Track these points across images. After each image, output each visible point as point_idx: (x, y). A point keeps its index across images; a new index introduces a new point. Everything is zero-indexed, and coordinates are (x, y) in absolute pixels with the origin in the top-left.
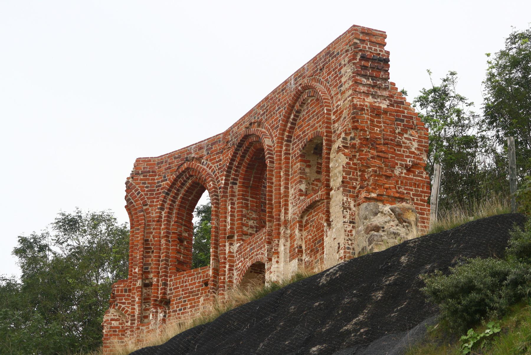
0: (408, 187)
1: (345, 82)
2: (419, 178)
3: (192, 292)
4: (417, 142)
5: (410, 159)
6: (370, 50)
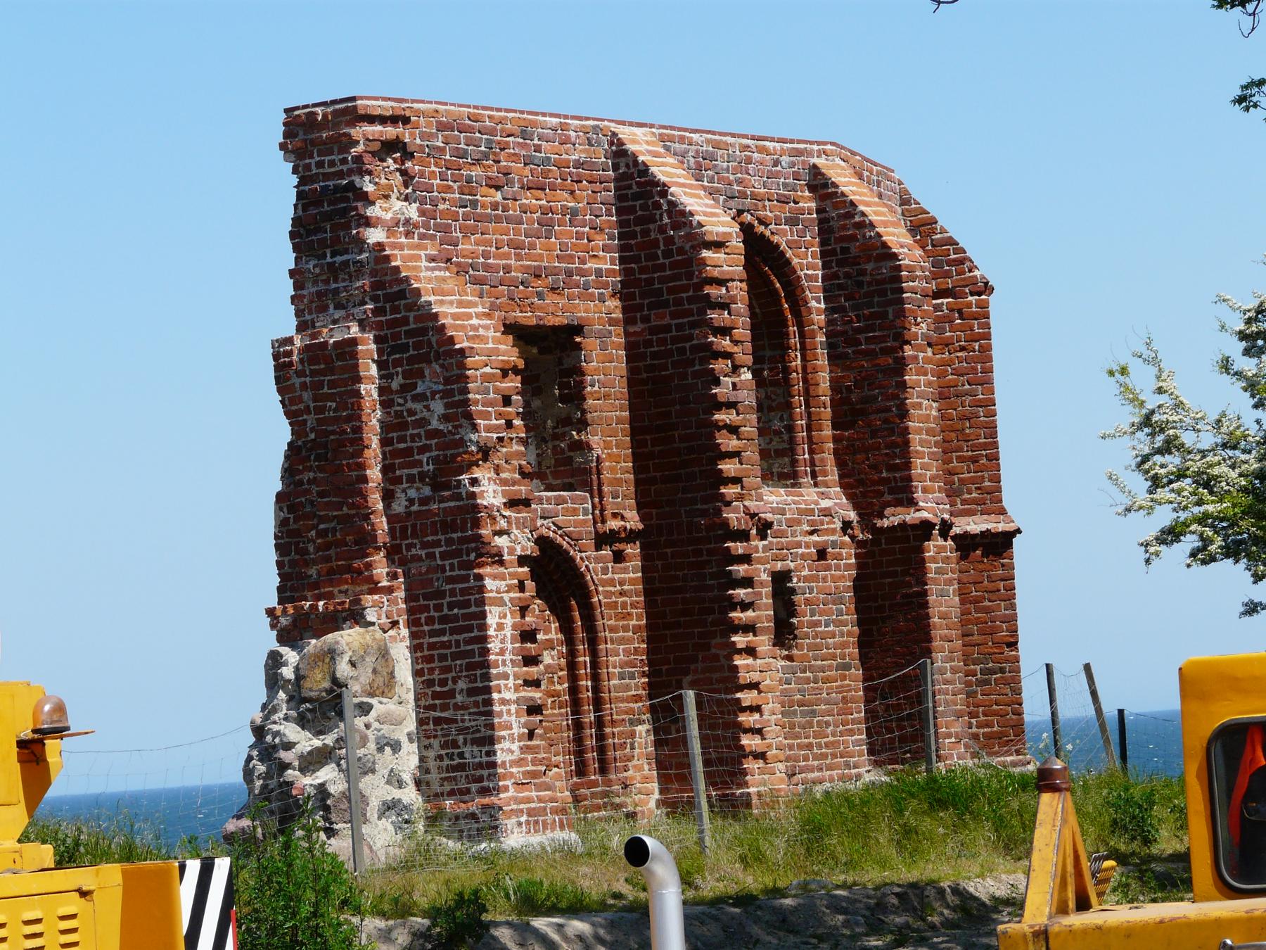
0: (430, 538)
2: (452, 504)
4: (441, 398)
5: (428, 454)
6: (321, 171)
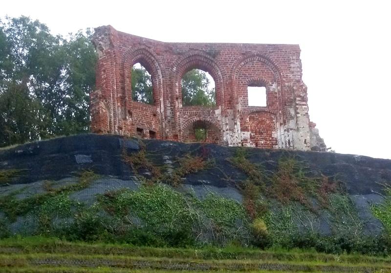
1: (293, 68)
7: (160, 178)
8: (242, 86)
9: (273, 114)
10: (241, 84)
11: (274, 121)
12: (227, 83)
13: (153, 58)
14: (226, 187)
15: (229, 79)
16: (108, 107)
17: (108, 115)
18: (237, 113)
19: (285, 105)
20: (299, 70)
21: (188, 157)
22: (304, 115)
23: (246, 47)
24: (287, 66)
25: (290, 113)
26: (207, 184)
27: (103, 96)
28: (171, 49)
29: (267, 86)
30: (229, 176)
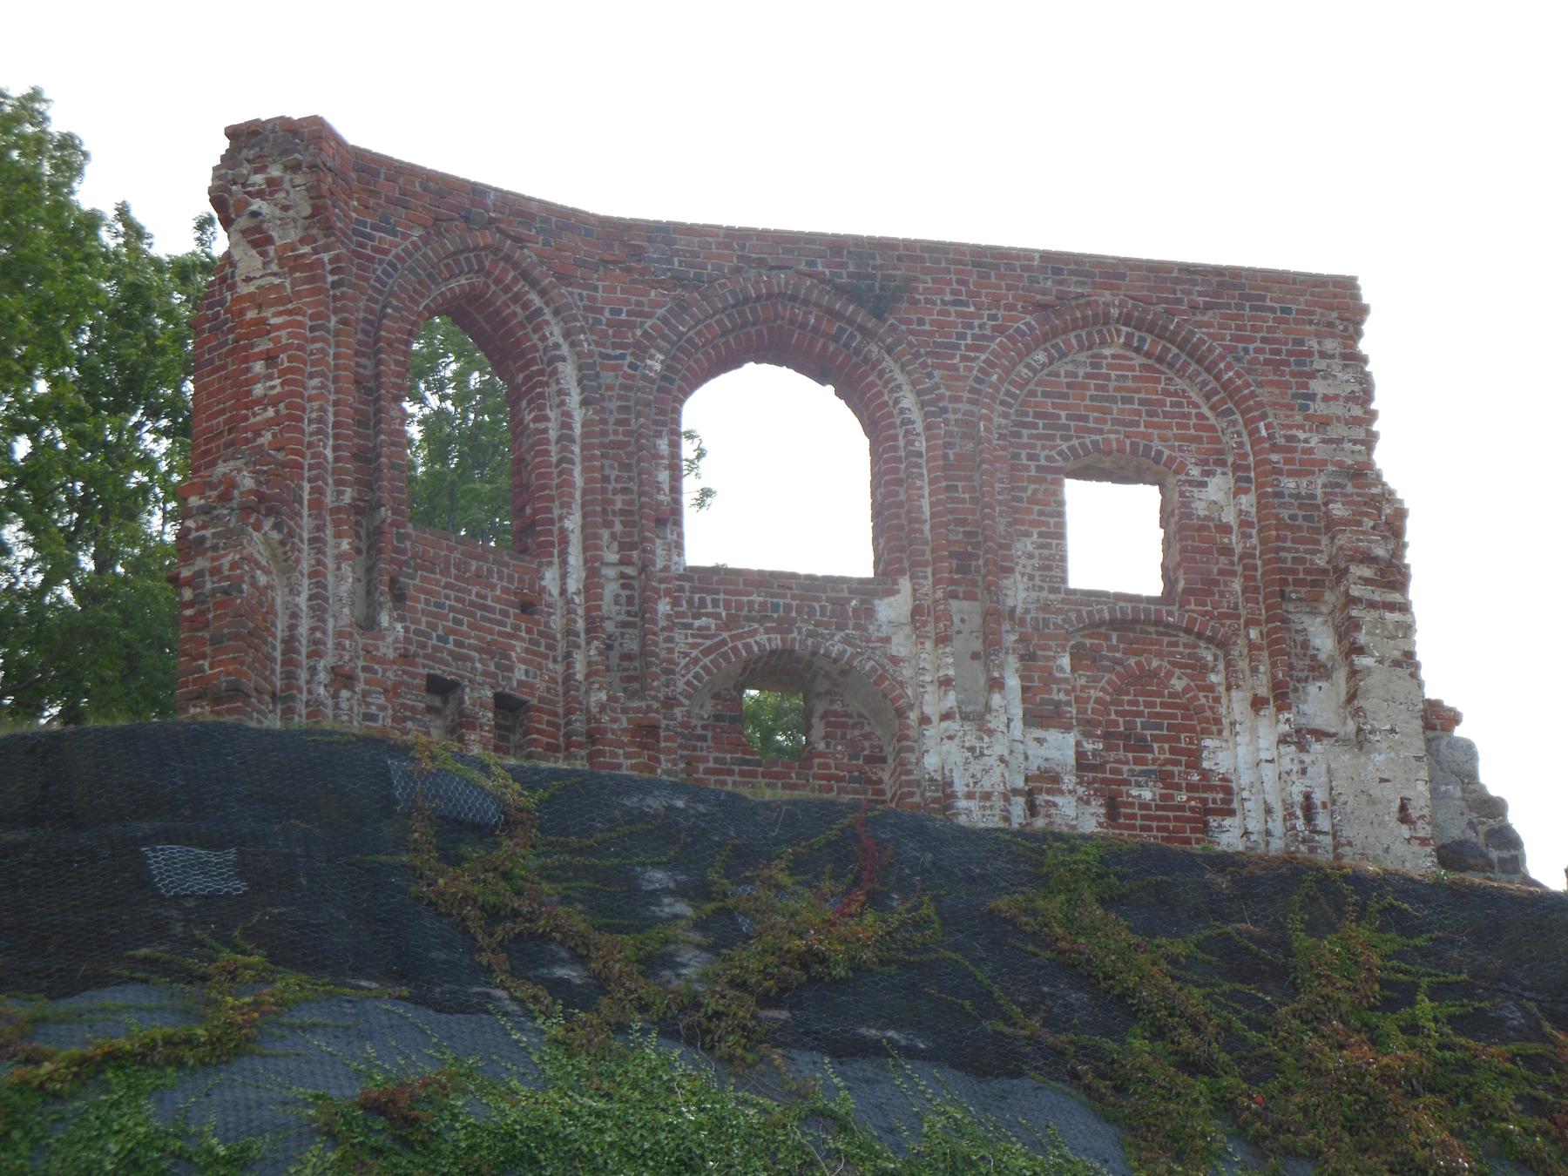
1: (1326, 398)
3: (485, 608)
7: (643, 1008)
8: (1031, 480)
9: (1210, 640)
10: (1027, 468)
11: (1213, 678)
12: (951, 454)
13: (537, 301)
14: (1018, 1074)
15: (964, 436)
16: (287, 565)
17: (279, 601)
18: (1006, 626)
19: (1282, 595)
20: (1357, 411)
21: (785, 879)
22: (1397, 663)
23: (1057, 272)
24: (1288, 385)
25: (1305, 645)
26: (910, 1053)
27: (262, 498)
28: (637, 253)
29: (1172, 480)
30: (1029, 1009)
